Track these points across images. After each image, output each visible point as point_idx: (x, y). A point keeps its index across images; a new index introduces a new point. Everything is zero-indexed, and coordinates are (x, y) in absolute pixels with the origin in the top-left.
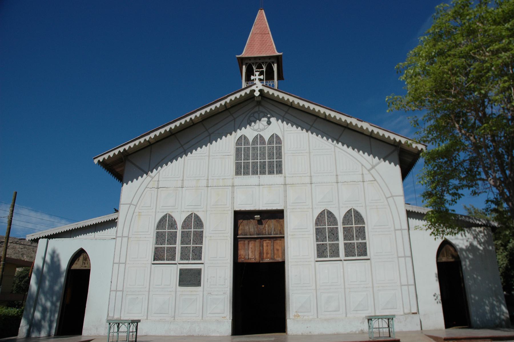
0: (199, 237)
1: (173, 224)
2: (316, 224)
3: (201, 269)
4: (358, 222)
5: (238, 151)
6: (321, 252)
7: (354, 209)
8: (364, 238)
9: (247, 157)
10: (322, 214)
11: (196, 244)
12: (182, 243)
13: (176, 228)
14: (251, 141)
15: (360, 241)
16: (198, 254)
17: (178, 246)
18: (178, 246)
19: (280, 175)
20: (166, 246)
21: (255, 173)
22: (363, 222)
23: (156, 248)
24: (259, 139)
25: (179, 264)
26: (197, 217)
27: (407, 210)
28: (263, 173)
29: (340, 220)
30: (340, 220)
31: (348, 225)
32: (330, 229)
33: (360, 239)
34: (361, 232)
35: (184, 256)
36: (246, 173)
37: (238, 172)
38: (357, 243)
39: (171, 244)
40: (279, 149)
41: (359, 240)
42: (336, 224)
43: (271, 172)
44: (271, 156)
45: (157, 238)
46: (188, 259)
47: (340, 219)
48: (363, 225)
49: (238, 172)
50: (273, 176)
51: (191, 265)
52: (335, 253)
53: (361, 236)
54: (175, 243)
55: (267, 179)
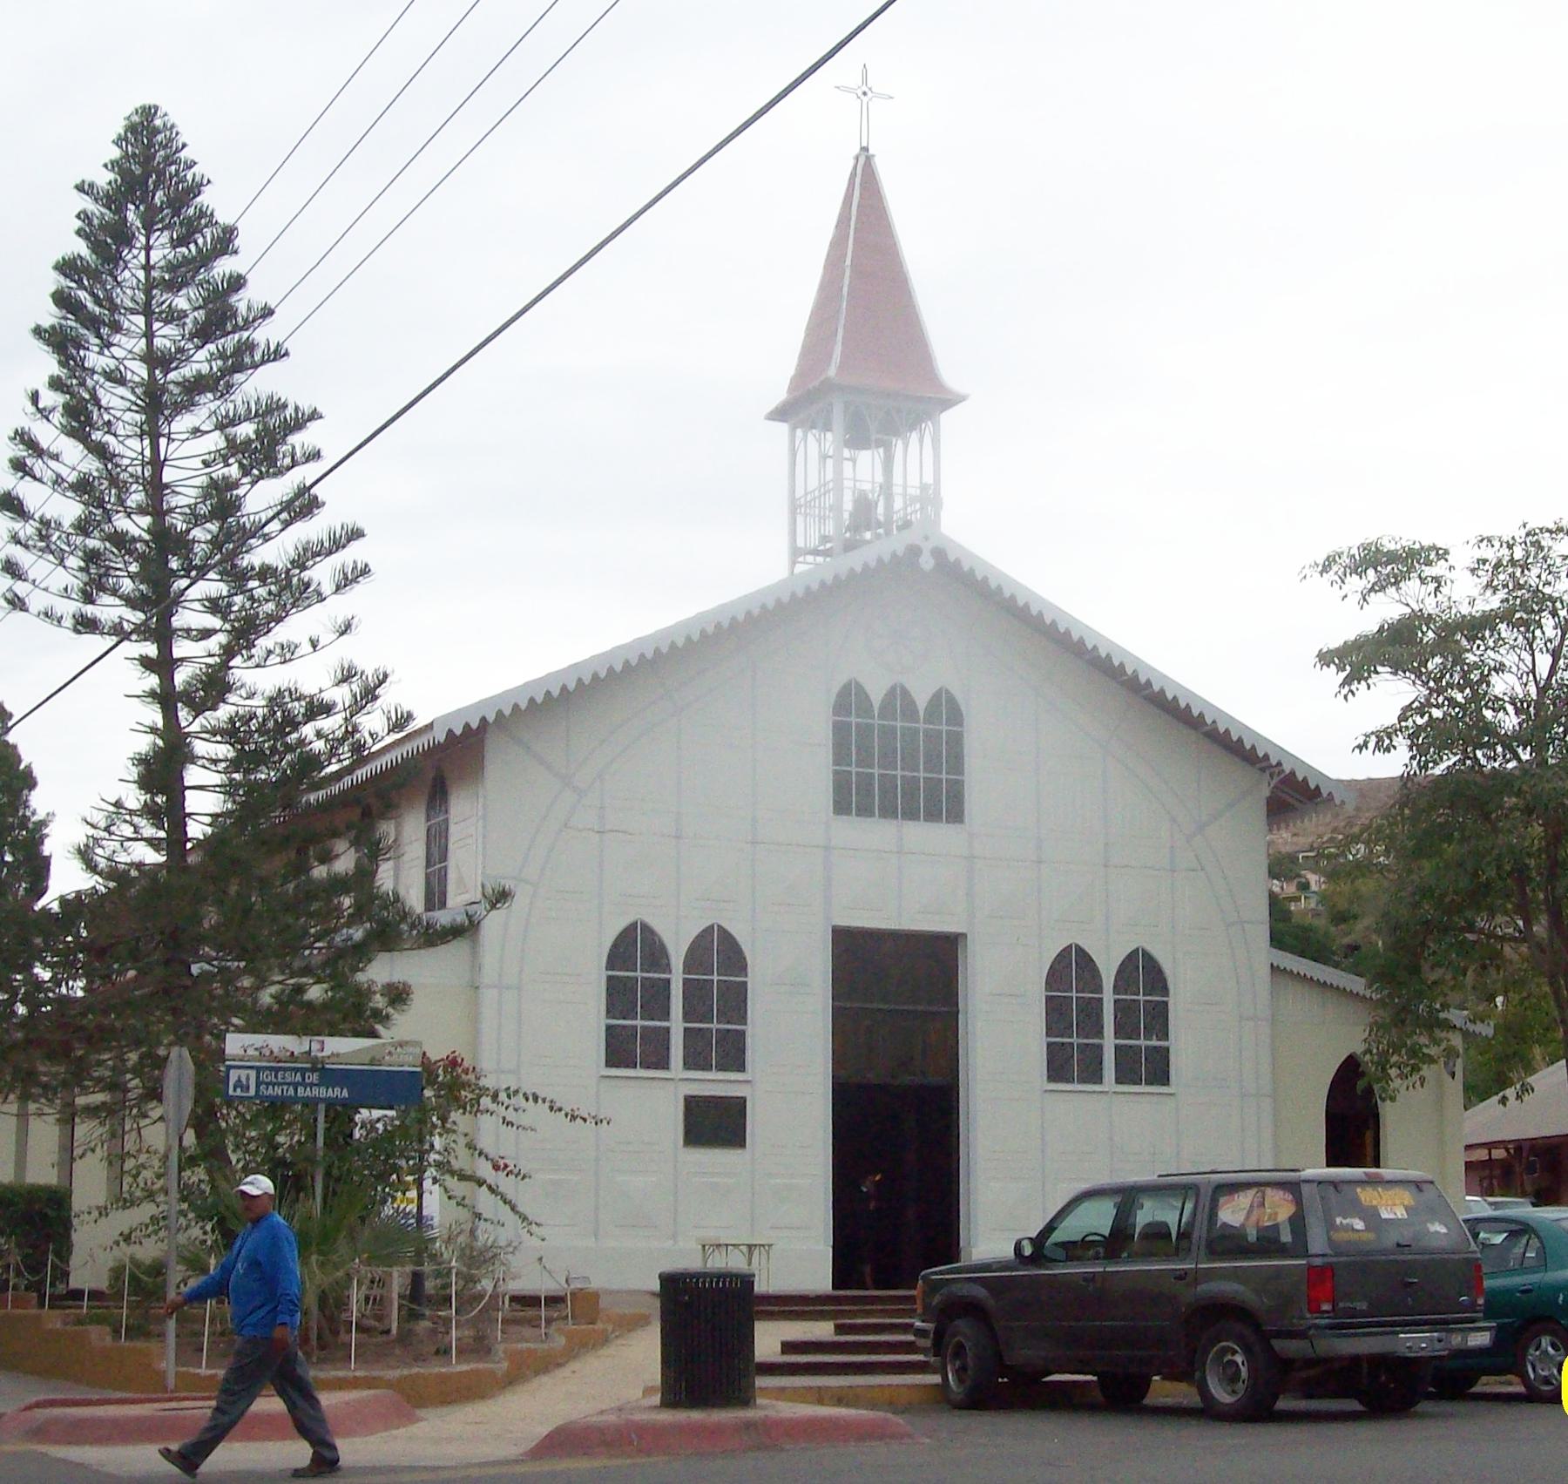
0: (736, 1001)
1: (656, 954)
2: (1049, 984)
3: (743, 1101)
4: (1152, 987)
5: (840, 731)
6: (1060, 1067)
7: (1143, 950)
8: (1166, 1036)
9: (864, 761)
10: (1064, 954)
11: (728, 1023)
12: (687, 1016)
13: (667, 968)
14: (876, 706)
15: (1154, 1043)
16: (733, 1054)
17: (677, 1024)
18: (677, 1024)
19: (958, 826)
20: (714, 1026)
21: (888, 812)
22: (1165, 990)
23: (609, 1028)
24: (899, 698)
25: (680, 1080)
26: (727, 939)
27: (1272, 965)
28: (911, 815)
29: (1108, 981)
30: (1108, 981)
31: (1126, 994)
32: (1081, 1001)
33: (1154, 1037)
34: (1159, 1019)
35: (696, 1060)
36: (865, 811)
37: (841, 806)
38: (1147, 1048)
39: (653, 1019)
40: (956, 741)
41: (1151, 1040)
42: (1099, 989)
43: (933, 815)
44: (933, 762)
45: (609, 995)
46: (708, 1067)
47: (1108, 977)
48: (1165, 999)
49: (841, 807)
50: (917, 823)
51: (715, 1083)
52: (1093, 1074)
53: (1158, 1027)
54: (666, 1015)
55: (919, 834)
